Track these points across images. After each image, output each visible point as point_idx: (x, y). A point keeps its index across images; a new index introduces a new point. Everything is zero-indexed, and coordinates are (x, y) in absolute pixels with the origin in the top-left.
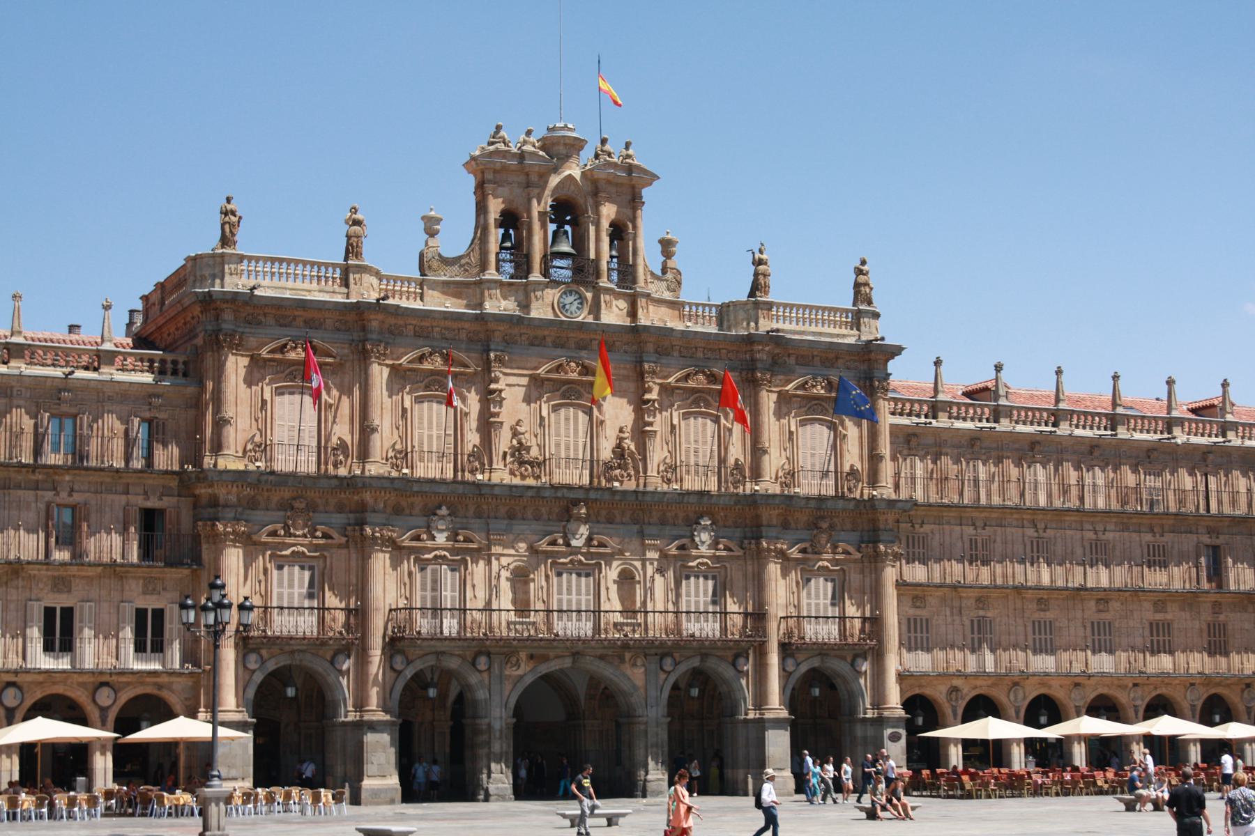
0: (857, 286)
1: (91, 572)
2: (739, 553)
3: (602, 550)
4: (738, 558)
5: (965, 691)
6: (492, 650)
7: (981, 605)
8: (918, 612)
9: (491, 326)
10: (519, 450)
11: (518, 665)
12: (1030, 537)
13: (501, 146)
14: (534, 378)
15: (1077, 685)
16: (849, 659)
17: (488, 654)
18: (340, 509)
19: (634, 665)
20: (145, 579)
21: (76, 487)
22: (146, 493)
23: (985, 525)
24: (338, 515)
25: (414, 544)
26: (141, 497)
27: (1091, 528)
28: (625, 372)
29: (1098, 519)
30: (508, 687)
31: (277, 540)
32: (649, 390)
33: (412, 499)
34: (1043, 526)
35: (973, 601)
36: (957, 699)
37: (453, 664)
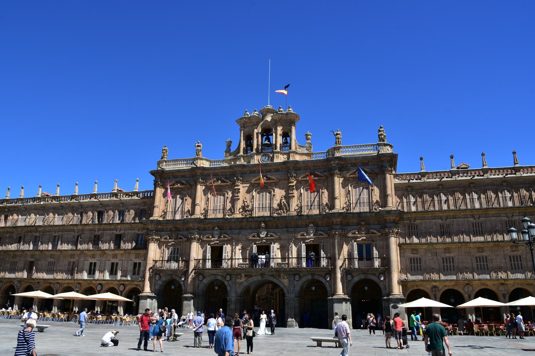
0: (379, 135)
1: (122, 252)
2: (327, 236)
3: (271, 238)
4: (327, 238)
5: (441, 287)
6: (231, 273)
7: (447, 251)
8: (415, 256)
9: (236, 169)
10: (243, 208)
11: (241, 278)
12: (471, 222)
13: (247, 116)
14: (251, 184)
15: (502, 284)
16: (377, 275)
17: (230, 275)
18: (187, 229)
19: (284, 278)
20: (136, 254)
21: (122, 229)
22: (139, 230)
23: (447, 218)
24: (187, 232)
25: (207, 239)
26: (137, 231)
27: (505, 215)
28: (284, 178)
29: (508, 211)
30: (238, 286)
31: (167, 240)
32: (293, 182)
33: (209, 225)
34: (478, 216)
35: (442, 250)
36: (435, 291)
37: (220, 278)
